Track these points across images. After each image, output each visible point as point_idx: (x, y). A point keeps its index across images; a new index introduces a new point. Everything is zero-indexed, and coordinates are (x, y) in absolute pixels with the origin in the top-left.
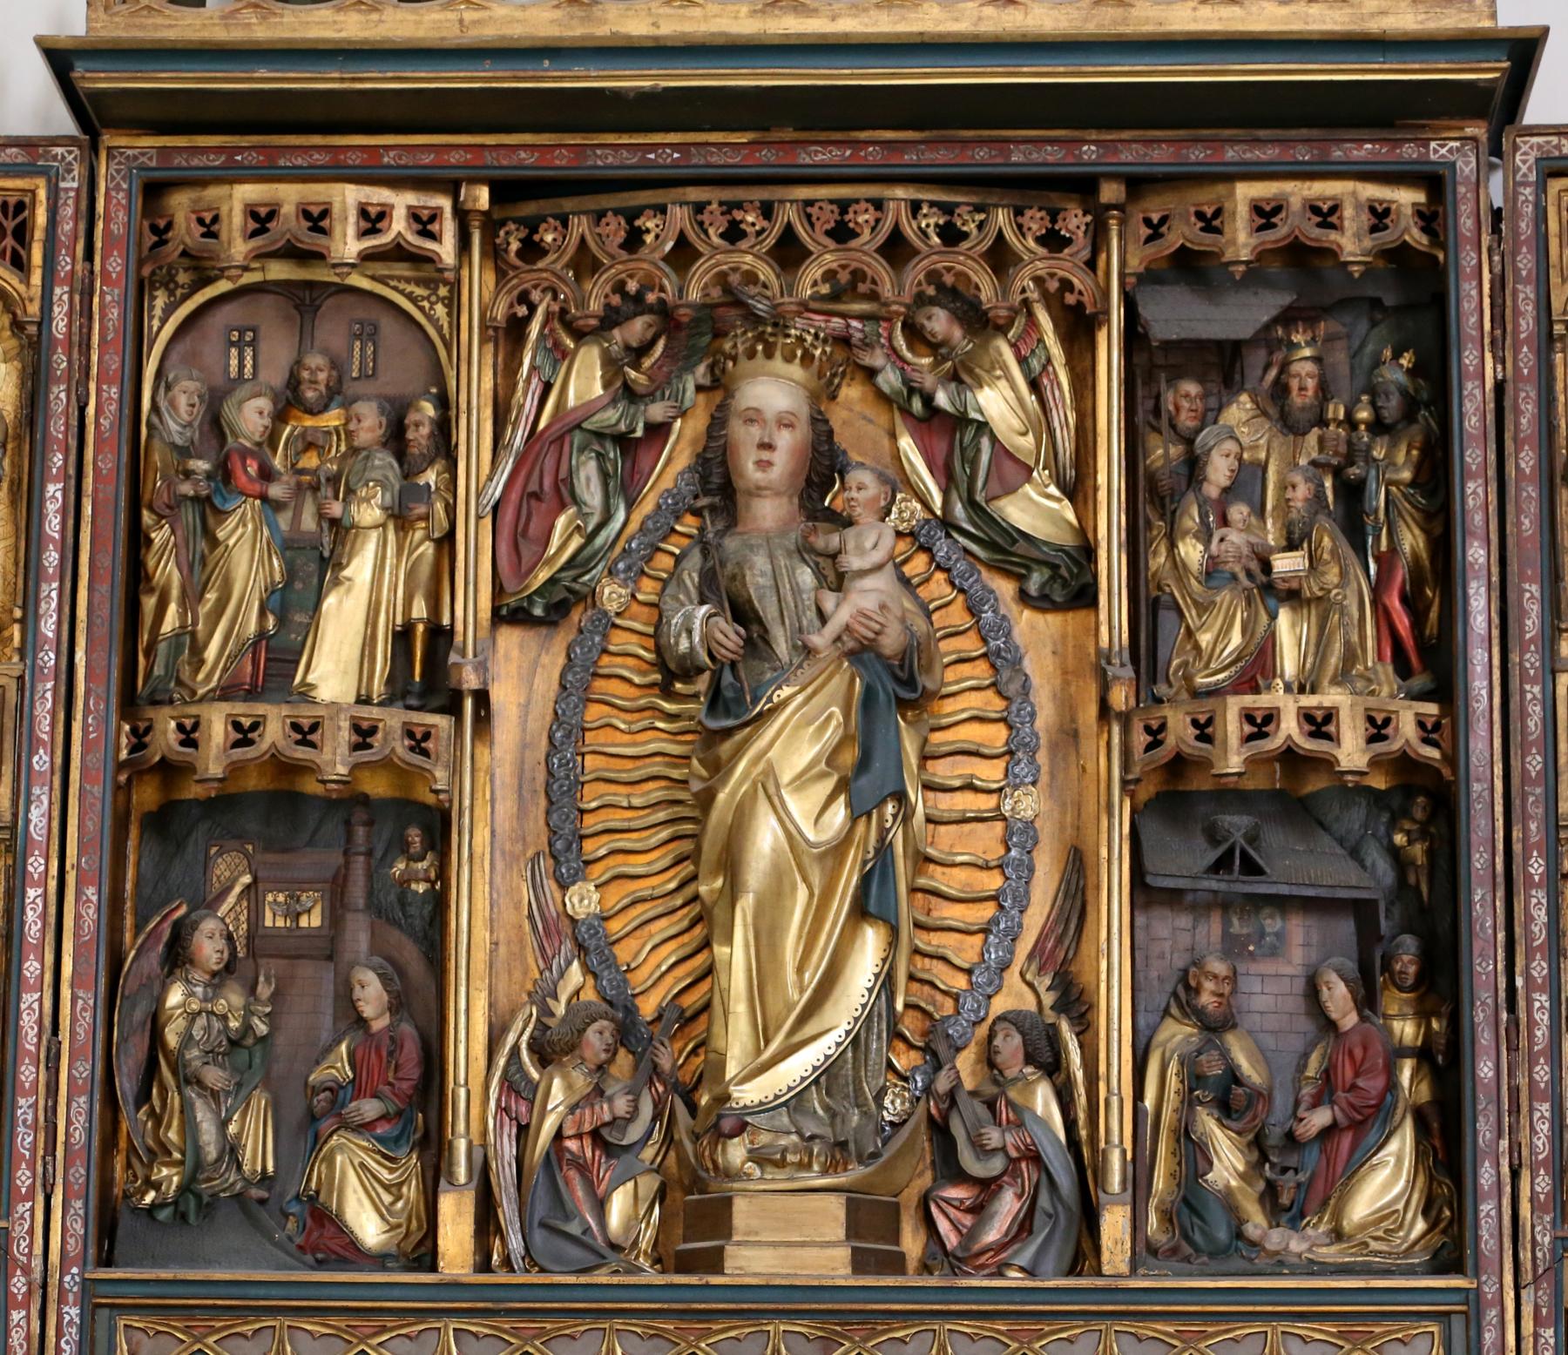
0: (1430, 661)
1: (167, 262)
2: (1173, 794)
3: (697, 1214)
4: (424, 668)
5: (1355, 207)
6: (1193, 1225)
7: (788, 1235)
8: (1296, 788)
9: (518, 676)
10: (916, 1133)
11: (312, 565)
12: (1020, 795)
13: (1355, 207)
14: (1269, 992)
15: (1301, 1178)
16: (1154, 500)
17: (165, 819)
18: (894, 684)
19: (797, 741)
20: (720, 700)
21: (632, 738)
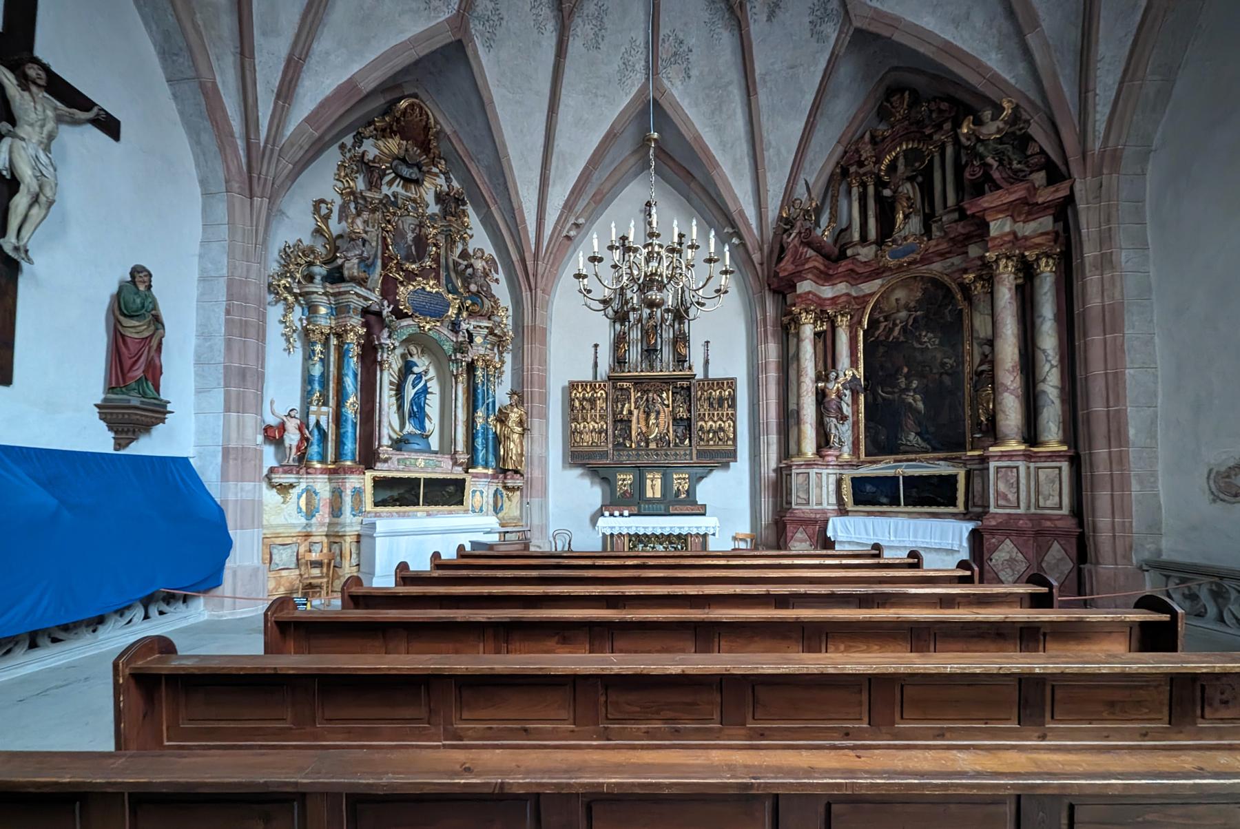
0: (690, 411)
1: (614, 387)
2: (674, 419)
3: (647, 445)
4: (630, 412)
5: (685, 383)
6: (676, 445)
7: (653, 446)
8: (681, 419)
9: (635, 412)
10: (661, 439)
11: (623, 406)
12: (665, 418)
13: (685, 383)
14: (680, 430)
15: (682, 442)
16: (673, 401)
17: (615, 422)
18: (658, 413)
19: (653, 416)
20: (648, 415)
21: (642, 416)
